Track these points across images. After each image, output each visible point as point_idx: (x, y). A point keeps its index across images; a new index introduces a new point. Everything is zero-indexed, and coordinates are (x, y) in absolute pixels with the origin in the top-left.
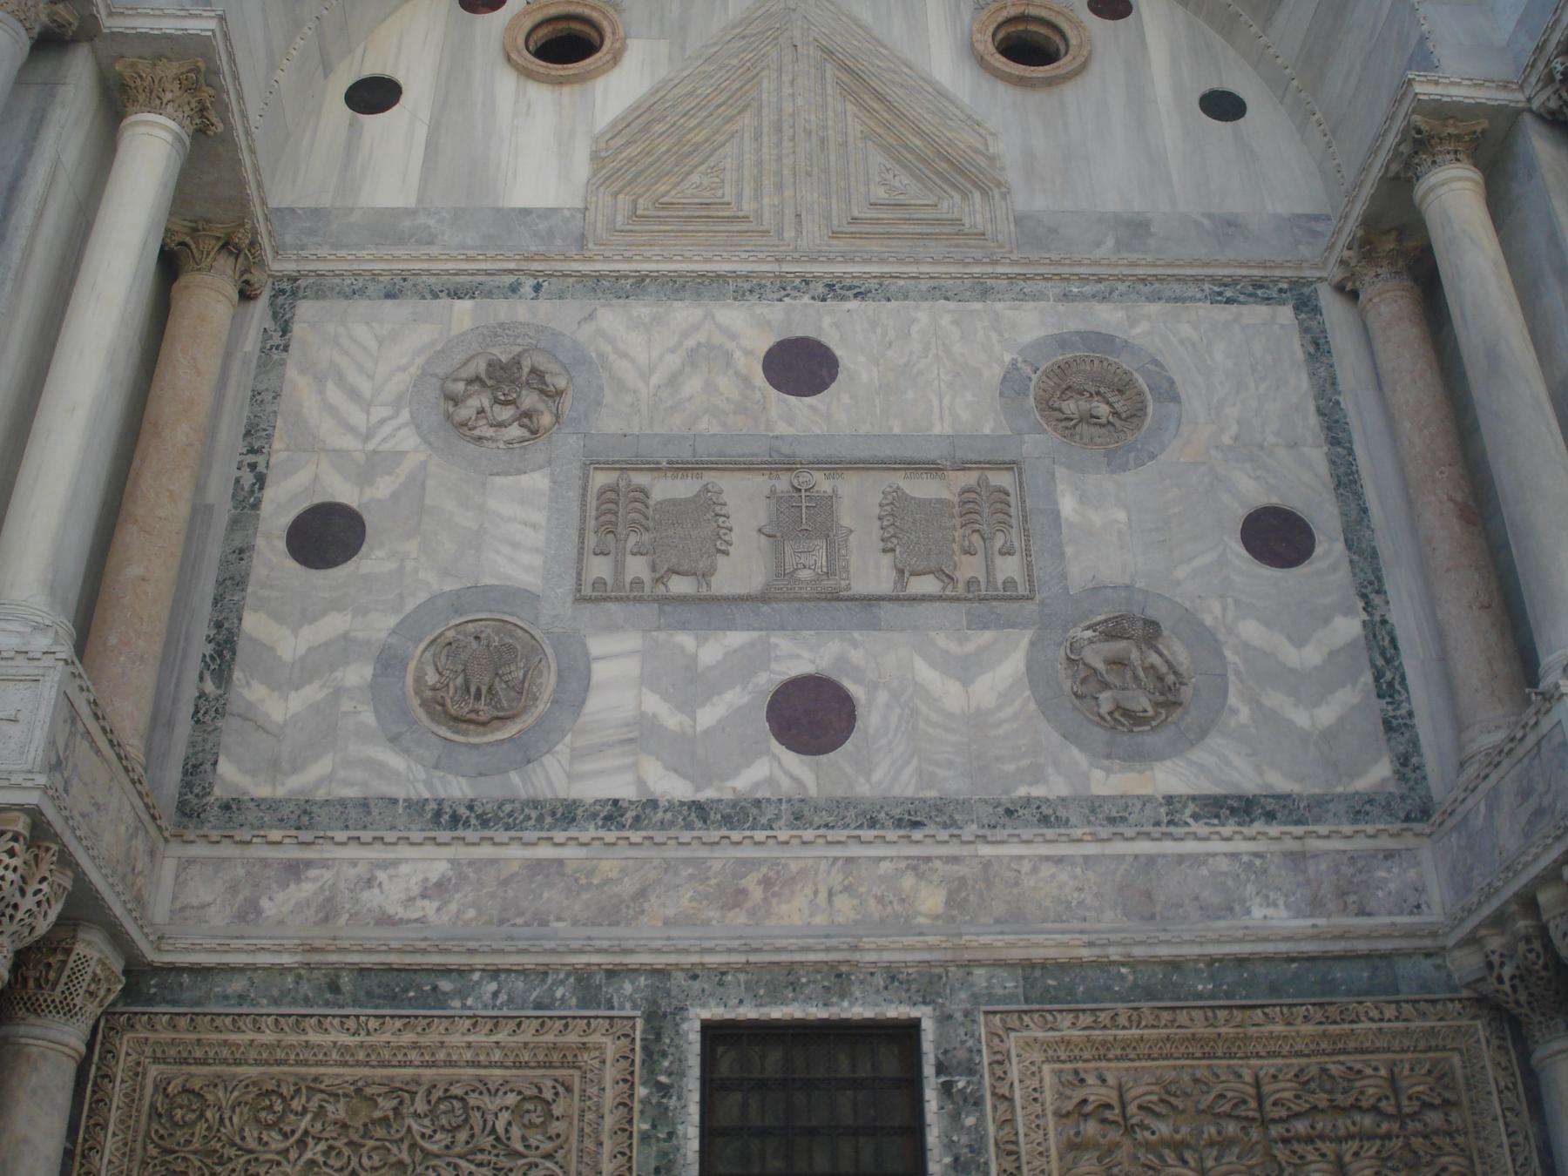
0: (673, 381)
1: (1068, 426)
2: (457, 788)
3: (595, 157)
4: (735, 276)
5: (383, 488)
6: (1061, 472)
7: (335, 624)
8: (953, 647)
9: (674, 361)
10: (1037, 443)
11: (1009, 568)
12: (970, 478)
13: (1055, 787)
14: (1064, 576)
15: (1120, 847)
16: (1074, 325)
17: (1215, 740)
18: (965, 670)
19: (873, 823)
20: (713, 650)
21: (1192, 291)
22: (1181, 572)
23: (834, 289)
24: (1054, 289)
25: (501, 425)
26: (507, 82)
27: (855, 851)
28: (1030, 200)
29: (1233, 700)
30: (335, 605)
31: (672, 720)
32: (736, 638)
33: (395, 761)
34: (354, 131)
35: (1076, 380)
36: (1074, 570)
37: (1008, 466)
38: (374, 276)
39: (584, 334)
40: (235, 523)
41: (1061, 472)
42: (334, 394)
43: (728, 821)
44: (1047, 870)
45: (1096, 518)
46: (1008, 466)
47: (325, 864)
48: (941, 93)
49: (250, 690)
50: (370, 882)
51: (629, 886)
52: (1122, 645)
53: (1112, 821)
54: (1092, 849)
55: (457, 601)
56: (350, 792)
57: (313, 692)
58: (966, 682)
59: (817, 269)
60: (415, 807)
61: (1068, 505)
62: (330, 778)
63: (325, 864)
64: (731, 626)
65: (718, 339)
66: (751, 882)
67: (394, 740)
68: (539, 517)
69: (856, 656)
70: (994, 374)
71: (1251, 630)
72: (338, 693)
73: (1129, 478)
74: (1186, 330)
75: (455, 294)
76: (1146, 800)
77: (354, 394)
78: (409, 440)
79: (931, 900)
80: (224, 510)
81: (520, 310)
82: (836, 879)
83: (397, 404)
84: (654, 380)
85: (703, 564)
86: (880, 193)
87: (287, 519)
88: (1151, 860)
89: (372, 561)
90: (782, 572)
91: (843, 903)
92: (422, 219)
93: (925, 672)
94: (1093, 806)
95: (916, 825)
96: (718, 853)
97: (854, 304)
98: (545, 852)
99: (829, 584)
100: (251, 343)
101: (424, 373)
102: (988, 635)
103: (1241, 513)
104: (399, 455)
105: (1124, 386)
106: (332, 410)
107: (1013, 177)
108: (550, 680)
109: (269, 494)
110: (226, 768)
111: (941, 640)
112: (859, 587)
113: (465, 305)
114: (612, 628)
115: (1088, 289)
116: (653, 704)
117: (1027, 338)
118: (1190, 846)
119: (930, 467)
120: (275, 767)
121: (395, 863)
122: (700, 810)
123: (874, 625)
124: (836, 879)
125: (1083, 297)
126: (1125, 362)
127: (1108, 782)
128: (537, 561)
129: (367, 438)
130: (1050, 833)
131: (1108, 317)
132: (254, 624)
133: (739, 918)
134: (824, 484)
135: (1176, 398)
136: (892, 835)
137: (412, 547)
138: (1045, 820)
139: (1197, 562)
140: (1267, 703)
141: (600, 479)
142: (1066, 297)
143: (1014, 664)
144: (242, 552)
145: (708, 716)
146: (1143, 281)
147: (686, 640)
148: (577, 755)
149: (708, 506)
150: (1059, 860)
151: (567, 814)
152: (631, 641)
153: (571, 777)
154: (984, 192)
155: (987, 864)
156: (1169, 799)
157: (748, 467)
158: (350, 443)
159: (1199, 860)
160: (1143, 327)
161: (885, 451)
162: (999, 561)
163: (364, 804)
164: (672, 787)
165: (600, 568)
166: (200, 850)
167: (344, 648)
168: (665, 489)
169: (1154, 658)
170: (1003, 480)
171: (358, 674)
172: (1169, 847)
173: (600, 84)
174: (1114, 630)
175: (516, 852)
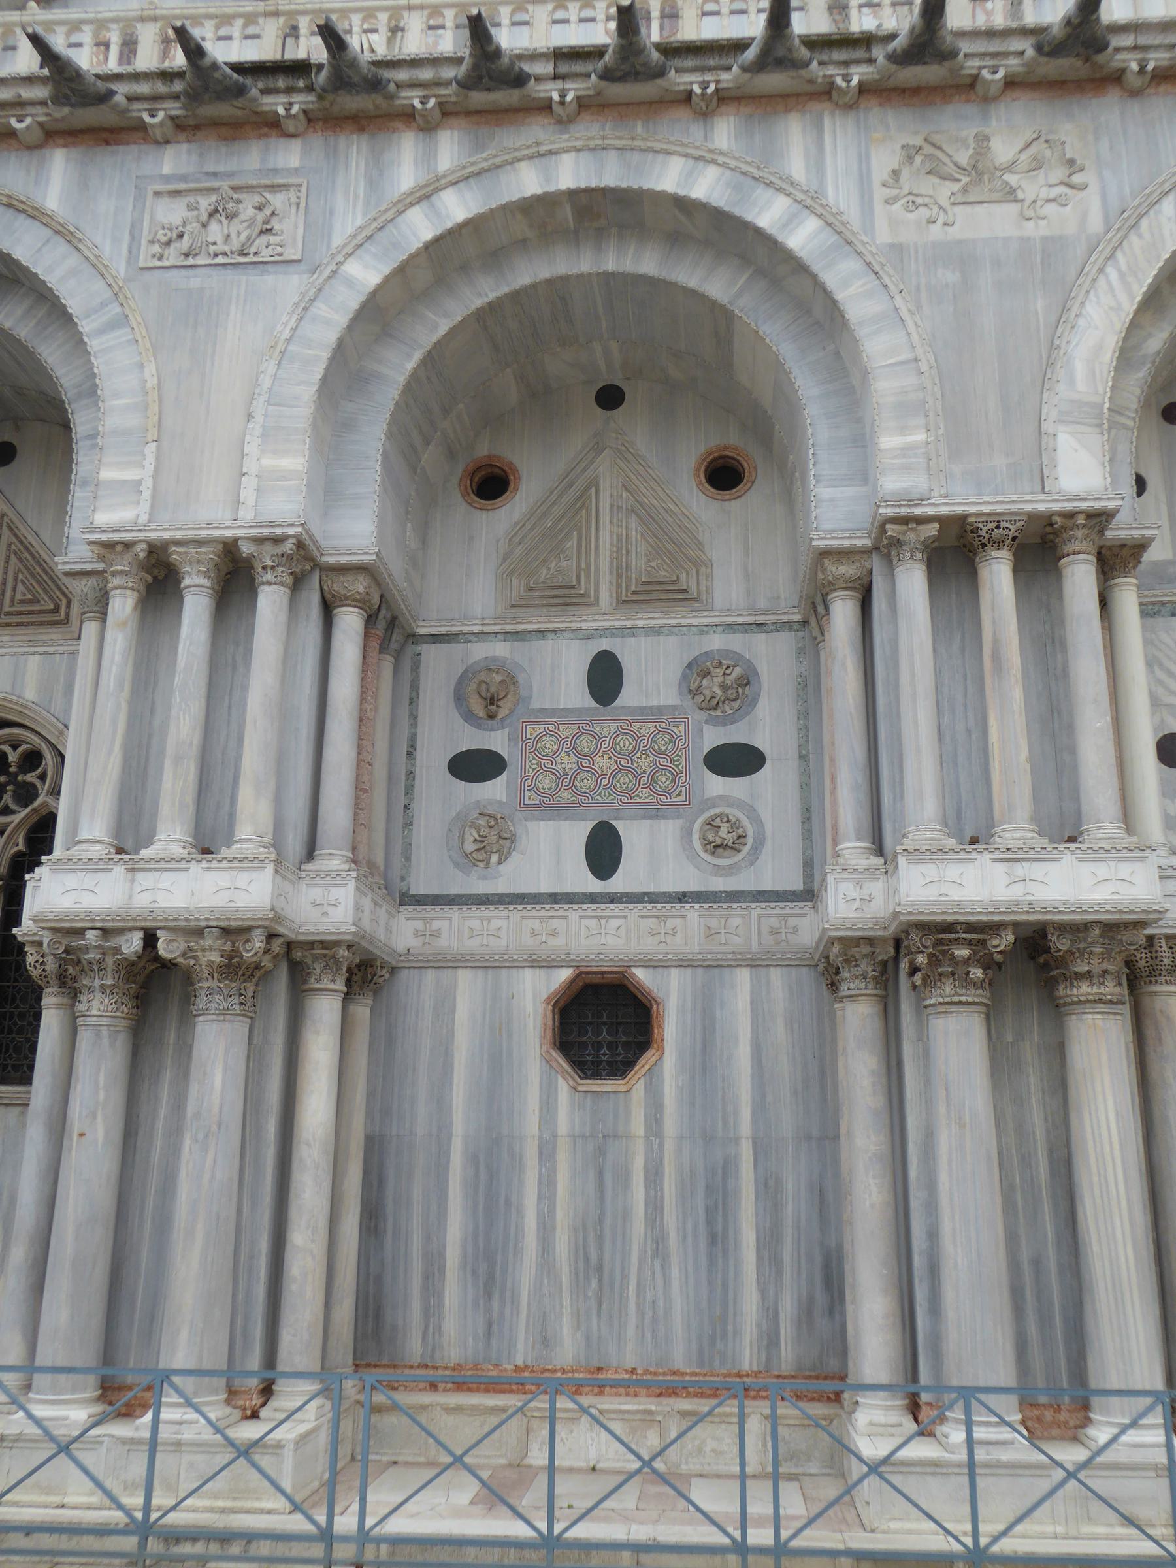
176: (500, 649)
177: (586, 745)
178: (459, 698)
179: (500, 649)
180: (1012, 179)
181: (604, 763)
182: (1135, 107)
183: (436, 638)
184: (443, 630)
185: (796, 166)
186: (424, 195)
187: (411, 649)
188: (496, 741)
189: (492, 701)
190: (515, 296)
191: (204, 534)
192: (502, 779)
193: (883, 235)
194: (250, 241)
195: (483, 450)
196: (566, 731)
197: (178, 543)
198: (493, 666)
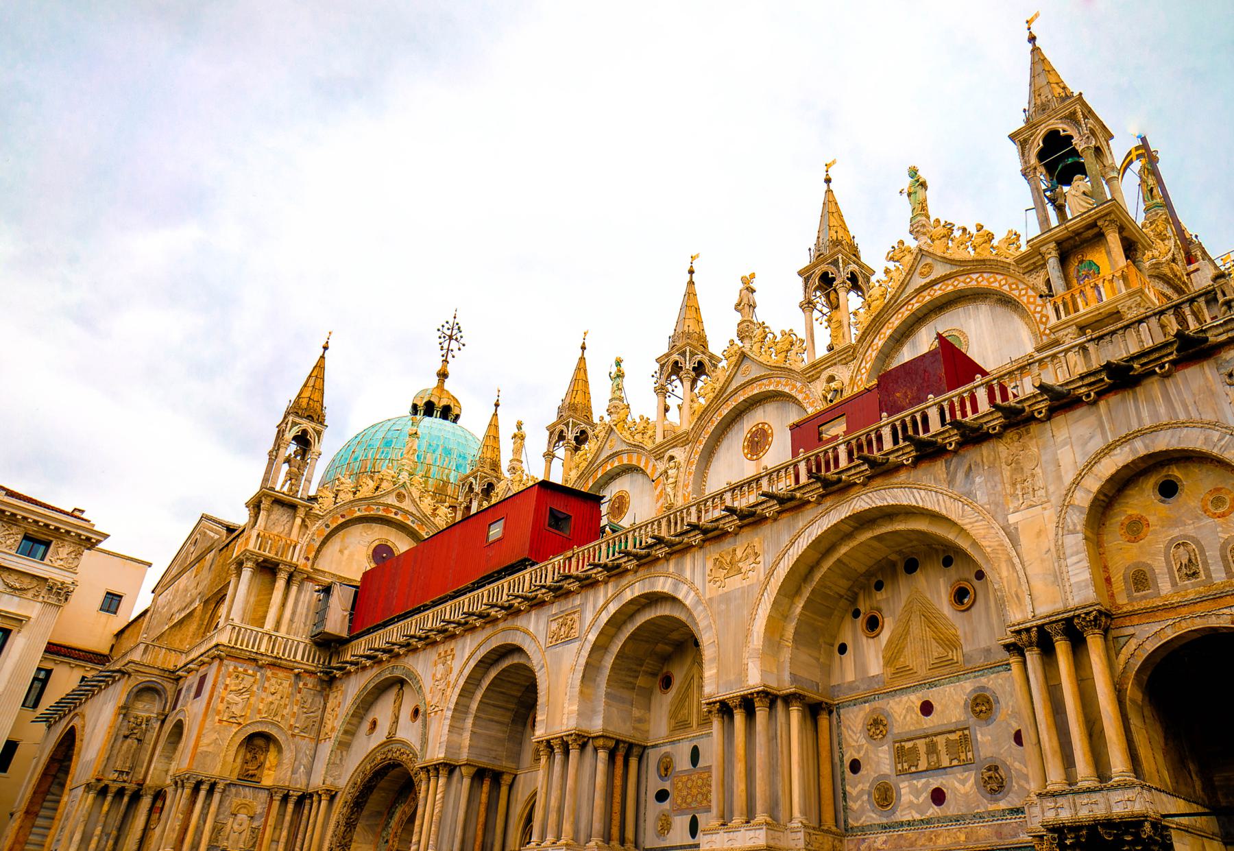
0: (905, 718)
1: (978, 714)
2: (884, 821)
3: (883, 657)
4: (910, 687)
5: (862, 754)
6: (977, 728)
7: (860, 786)
8: (961, 778)
9: (904, 711)
10: (972, 720)
11: (970, 755)
12: (961, 733)
13: (982, 810)
14: (979, 756)
15: (995, 822)
16: (977, 685)
17: (1010, 794)
18: (963, 782)
19: (951, 821)
20: (920, 783)
21: (1001, 668)
22: (1002, 751)
23: (932, 685)
24: (972, 675)
25: (878, 735)
26: (864, 639)
27: (949, 827)
28: (966, 649)
29: (1014, 784)
30: (859, 783)
31: (915, 801)
32: (923, 780)
33: (874, 816)
34: (841, 658)
35: (978, 701)
36: (981, 754)
37: (966, 729)
38: (851, 701)
39: (888, 708)
40: (841, 766)
41: (977, 728)
42: (850, 732)
43: (927, 823)
44: (982, 828)
45: (985, 739)
46: (966, 729)
47: (868, 838)
48: (946, 618)
49: (850, 803)
50: (875, 842)
51: (914, 839)
52: (990, 773)
53: (993, 816)
54: (990, 823)
55: (876, 779)
56: (869, 823)
57: (859, 802)
58: (964, 786)
59: (926, 681)
60: (879, 825)
61: (979, 736)
62: (864, 821)
63: (868, 838)
64: (922, 778)
65: (911, 704)
66: (933, 836)
67: (873, 811)
68: (887, 756)
69: (944, 782)
70: (962, 703)
71: (1017, 764)
72: (863, 802)
73: (990, 727)
74: (1000, 681)
75: (865, 703)
76: (998, 810)
77: (853, 731)
78: (864, 741)
79: (963, 838)
80: (839, 763)
81: (876, 704)
82: (947, 834)
83: (860, 733)
84: (902, 717)
85: (916, 764)
86: (936, 655)
87: (848, 764)
88: (1001, 824)
89: (863, 772)
90: (929, 764)
91: (948, 839)
92: (857, 683)
93: (957, 784)
94: (989, 812)
95: (958, 821)
96: (928, 830)
97: (934, 689)
98: (900, 833)
99: (937, 765)
100: (835, 722)
101: (864, 724)
102: (966, 774)
103: (1014, 732)
104: (863, 745)
105: (988, 701)
106: (850, 736)
107: (962, 642)
108: (895, 794)
109: (845, 758)
110: (850, 820)
111: (959, 775)
112: (944, 766)
113: (867, 705)
114: (903, 781)
115: (979, 673)
116: (912, 798)
117: (968, 691)
118: (1008, 821)
119: (954, 732)
120: (857, 820)
121: (877, 838)
122: (922, 820)
123: (946, 774)
124: (947, 834)
125: (978, 676)
126: (987, 694)
127: (992, 807)
128: (888, 767)
129: (857, 742)
130: (981, 820)
131: (984, 680)
132: (848, 788)
133: (932, 844)
134: (935, 739)
135: (999, 702)
136: (954, 823)
137: (868, 767)
138: (980, 817)
139: (1006, 748)
140: (1021, 783)
141: (897, 745)
142: (975, 677)
143: (972, 780)
144: (843, 772)
145: (921, 800)
146: (991, 668)
147: (915, 782)
148: (902, 811)
149: (915, 748)
150: (984, 826)
151: (901, 824)
152: (906, 784)
153: (902, 816)
154: (957, 650)
155: (972, 828)
156: (1003, 810)
157: (920, 738)
158: (854, 744)
159: (1010, 824)
160: (991, 682)
161: (944, 729)
162: (968, 754)
163: (871, 825)
164: (917, 817)
165: (899, 767)
166: (849, 838)
167: (862, 792)
168: (908, 745)
169: (997, 776)
170: (966, 732)
171: (865, 797)
172: (1004, 821)
173: (881, 635)
174: (989, 769)
175: (895, 833)
176: (668, 749)
177: (689, 785)
178: (658, 769)
179: (668, 749)
180: (740, 565)
181: (694, 791)
182: (775, 525)
183: (653, 746)
184: (654, 743)
185: (688, 574)
186: (605, 607)
187: (647, 751)
188: (667, 786)
189: (666, 769)
190: (638, 629)
191: (556, 736)
192: (668, 800)
193: (707, 597)
194: (568, 633)
195: (665, 670)
196: (685, 779)
197: (552, 739)
198: (667, 755)
